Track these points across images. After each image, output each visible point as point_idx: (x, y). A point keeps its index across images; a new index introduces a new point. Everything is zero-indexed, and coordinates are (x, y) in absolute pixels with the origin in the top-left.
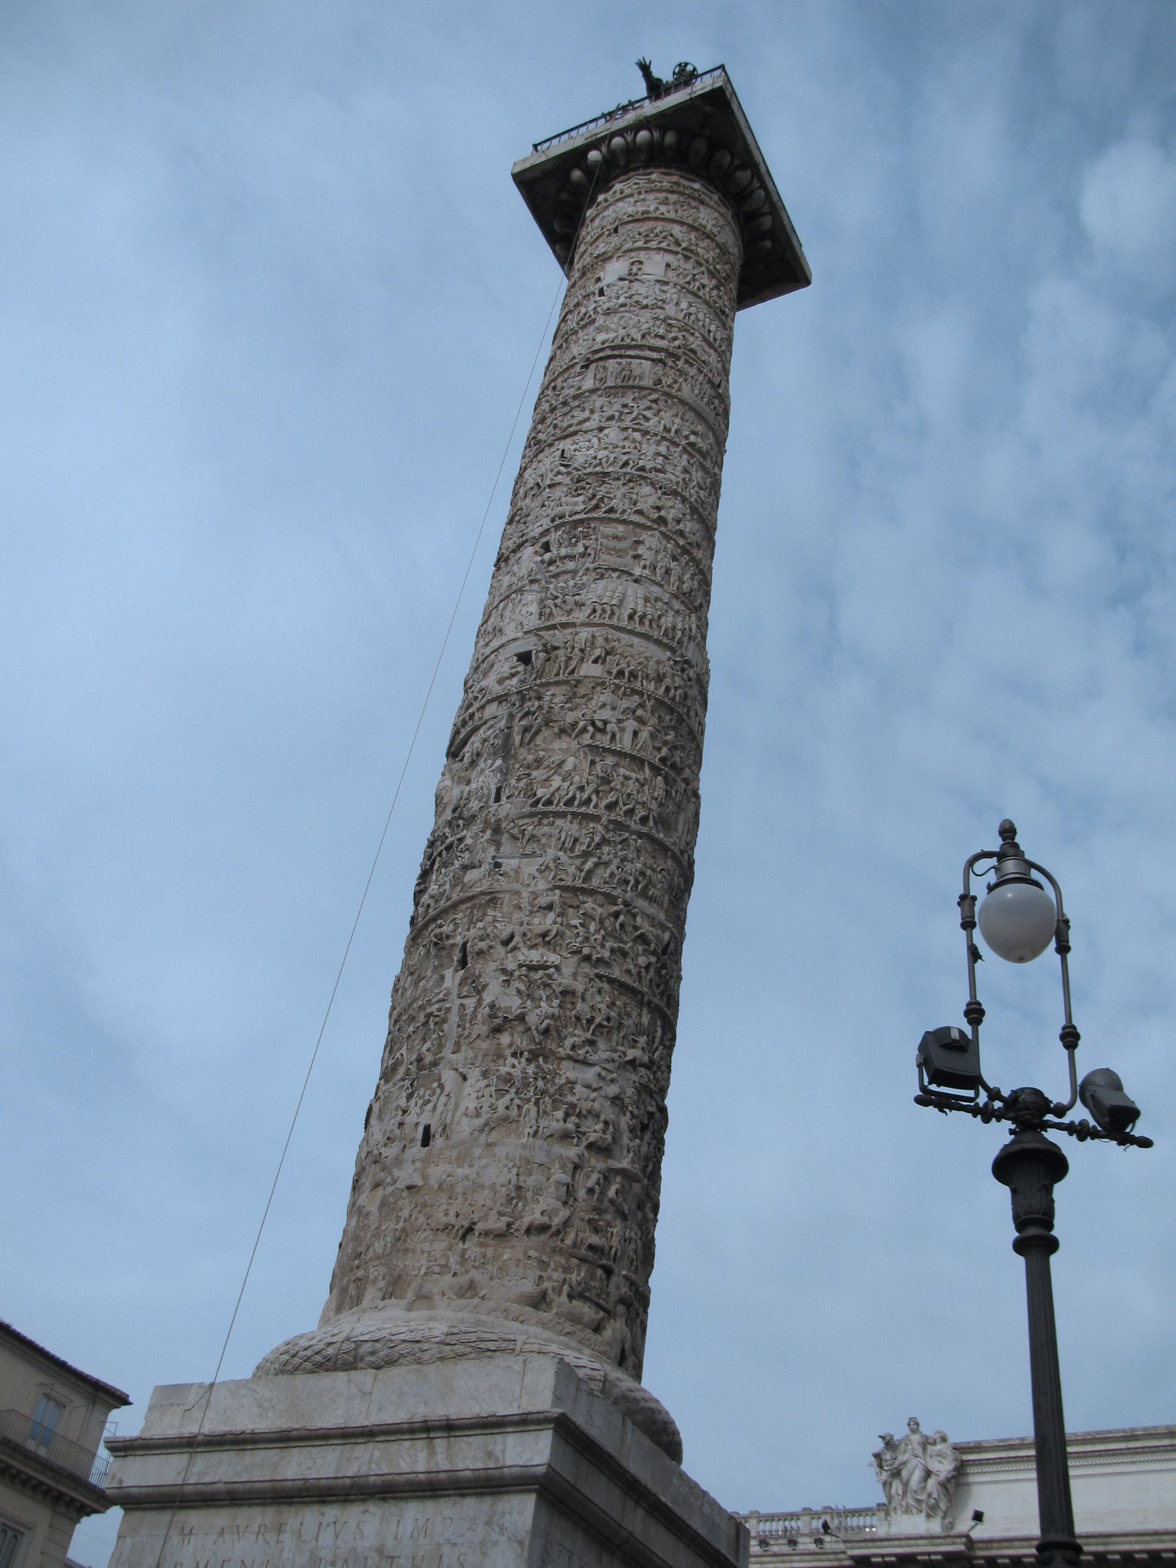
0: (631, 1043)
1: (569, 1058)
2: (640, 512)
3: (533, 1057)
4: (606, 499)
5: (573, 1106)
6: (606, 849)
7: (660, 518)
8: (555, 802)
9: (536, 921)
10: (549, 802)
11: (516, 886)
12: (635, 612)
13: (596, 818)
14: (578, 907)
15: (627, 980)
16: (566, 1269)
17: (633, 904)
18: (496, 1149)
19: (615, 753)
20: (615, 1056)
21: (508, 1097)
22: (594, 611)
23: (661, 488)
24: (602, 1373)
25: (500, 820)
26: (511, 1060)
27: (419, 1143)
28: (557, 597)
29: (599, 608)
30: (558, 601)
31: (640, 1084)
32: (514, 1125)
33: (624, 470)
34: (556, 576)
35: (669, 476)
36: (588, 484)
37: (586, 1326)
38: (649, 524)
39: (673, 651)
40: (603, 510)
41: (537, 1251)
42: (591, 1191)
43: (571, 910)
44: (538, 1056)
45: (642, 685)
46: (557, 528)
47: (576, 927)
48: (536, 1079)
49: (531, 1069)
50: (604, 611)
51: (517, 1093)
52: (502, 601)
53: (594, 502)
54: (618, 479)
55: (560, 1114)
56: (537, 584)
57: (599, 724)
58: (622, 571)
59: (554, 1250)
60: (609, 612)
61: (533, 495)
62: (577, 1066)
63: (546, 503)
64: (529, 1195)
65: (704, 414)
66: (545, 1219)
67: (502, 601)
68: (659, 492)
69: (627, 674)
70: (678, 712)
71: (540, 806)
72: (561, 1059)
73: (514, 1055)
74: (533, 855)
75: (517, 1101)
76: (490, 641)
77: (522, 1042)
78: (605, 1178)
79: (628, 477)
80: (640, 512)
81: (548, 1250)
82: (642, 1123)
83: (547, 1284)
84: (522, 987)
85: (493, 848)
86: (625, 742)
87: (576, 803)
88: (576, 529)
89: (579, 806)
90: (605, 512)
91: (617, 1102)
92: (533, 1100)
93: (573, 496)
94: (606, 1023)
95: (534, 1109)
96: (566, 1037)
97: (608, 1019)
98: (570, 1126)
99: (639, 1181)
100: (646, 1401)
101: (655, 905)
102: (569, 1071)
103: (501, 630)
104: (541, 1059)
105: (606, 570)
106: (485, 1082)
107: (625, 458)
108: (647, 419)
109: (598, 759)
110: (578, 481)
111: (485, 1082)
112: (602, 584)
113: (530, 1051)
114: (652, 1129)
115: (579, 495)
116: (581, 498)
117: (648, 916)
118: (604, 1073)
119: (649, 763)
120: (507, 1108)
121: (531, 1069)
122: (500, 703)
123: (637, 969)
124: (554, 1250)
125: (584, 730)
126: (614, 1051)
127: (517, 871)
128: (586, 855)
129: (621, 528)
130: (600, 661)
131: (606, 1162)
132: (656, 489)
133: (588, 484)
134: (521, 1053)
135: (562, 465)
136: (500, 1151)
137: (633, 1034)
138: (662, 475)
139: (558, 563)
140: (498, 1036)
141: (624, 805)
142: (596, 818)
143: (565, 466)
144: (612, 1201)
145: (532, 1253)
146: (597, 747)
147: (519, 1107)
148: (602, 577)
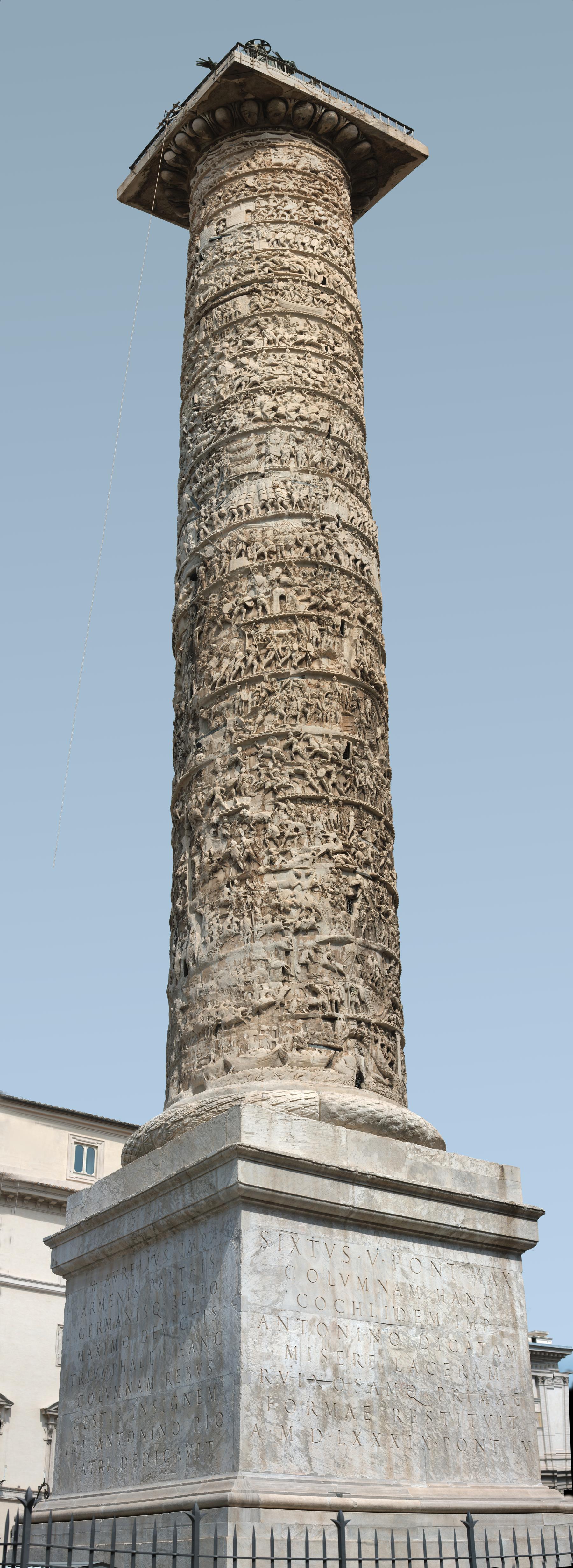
0: (324, 839)
1: (269, 871)
3: (242, 880)
5: (278, 907)
6: (272, 698)
8: (227, 680)
9: (228, 777)
10: (223, 682)
11: (211, 756)
13: (260, 679)
14: (257, 753)
15: (309, 792)
16: (293, 1030)
17: (303, 733)
18: (226, 961)
19: (265, 621)
20: (308, 855)
21: (228, 920)
23: (274, 392)
24: (317, 1099)
25: (195, 710)
26: (227, 890)
27: (183, 974)
31: (337, 868)
32: (236, 938)
33: (240, 391)
35: (281, 378)
37: (315, 1066)
38: (266, 425)
39: (309, 516)
41: (267, 1024)
42: (304, 965)
43: (252, 758)
44: (245, 879)
45: (283, 557)
47: (258, 770)
48: (246, 897)
49: (242, 890)
51: (235, 913)
55: (268, 917)
57: (249, 604)
58: (249, 473)
59: (281, 1019)
62: (277, 875)
64: (256, 986)
65: (307, 313)
66: (271, 999)
69: (266, 554)
70: (322, 563)
71: (217, 687)
72: (262, 874)
73: (228, 886)
74: (218, 728)
75: (236, 919)
77: (232, 873)
78: (316, 951)
81: (276, 1020)
82: (347, 897)
83: (279, 1046)
84: (225, 832)
85: (194, 734)
86: (275, 609)
87: (243, 672)
89: (246, 673)
91: (316, 890)
92: (246, 914)
94: (295, 833)
95: (248, 920)
96: (263, 857)
97: (297, 830)
98: (278, 923)
99: (351, 942)
100: (364, 1107)
101: (326, 724)
102: (270, 881)
104: (247, 882)
106: (213, 913)
108: (251, 343)
109: (253, 632)
111: (213, 913)
113: (238, 879)
114: (361, 897)
117: (322, 735)
118: (299, 871)
119: (299, 616)
120: (229, 927)
121: (242, 890)
122: (185, 618)
123: (318, 781)
124: (281, 1019)
125: (240, 613)
126: (308, 851)
127: (210, 745)
128: (255, 712)
129: (244, 440)
130: (243, 554)
131: (313, 939)
132: (270, 394)
134: (233, 882)
136: (229, 962)
137: (323, 832)
140: (216, 875)
141: (281, 657)
142: (260, 679)
144: (325, 966)
145: (264, 1027)
146: (250, 623)
147: (238, 923)
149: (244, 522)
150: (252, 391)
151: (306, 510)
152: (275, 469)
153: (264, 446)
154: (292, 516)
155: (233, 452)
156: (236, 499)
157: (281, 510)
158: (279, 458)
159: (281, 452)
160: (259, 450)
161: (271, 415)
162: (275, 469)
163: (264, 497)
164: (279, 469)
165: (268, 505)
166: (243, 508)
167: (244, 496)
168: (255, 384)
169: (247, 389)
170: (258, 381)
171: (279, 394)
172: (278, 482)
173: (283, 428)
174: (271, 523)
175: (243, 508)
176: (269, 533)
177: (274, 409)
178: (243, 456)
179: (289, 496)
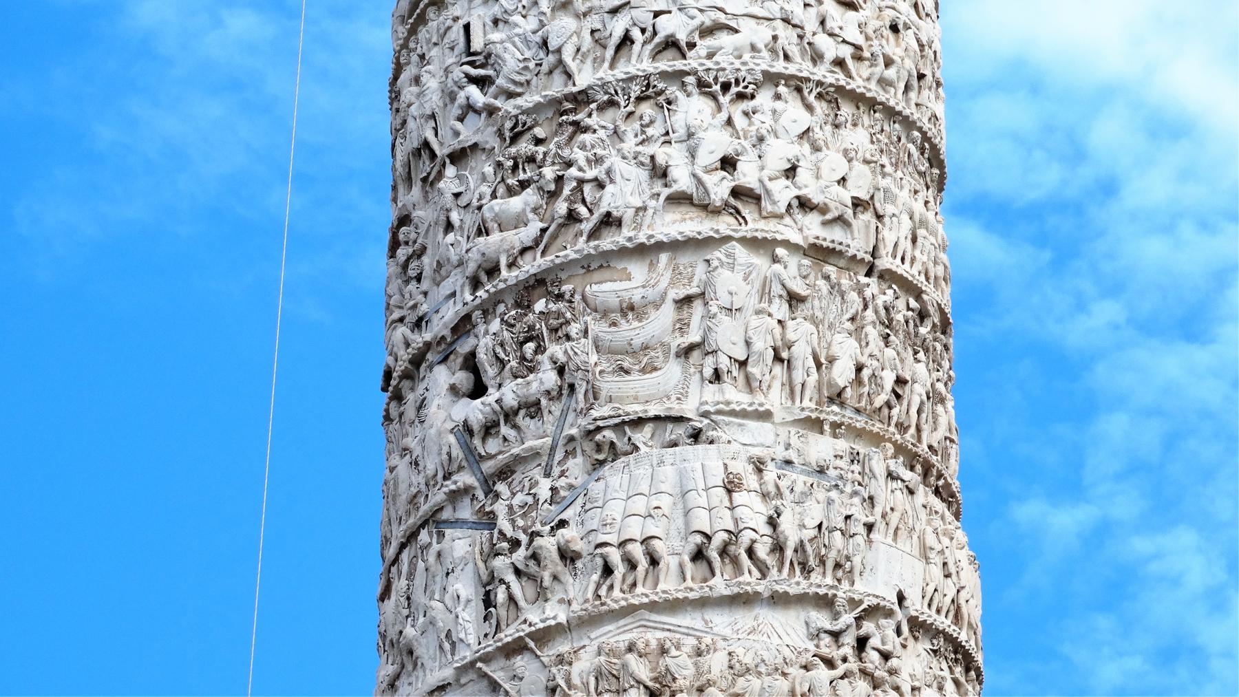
2: (680, 199)
4: (587, 188)
7: (736, 192)
12: (709, 537)
22: (608, 571)
23: (726, 87)
28: (515, 544)
29: (615, 556)
30: (521, 553)
34: (505, 473)
36: (538, 141)
40: (586, 227)
46: (487, 310)
50: (632, 565)
52: (403, 546)
53: (562, 207)
54: (612, 103)
56: (467, 501)
58: (657, 418)
60: (643, 563)
61: (424, 180)
63: (455, 217)
67: (403, 546)
68: (725, 100)
76: (397, 677)
79: (636, 90)
80: (680, 199)
88: (529, 307)
90: (594, 234)
93: (511, 192)
103: (411, 652)
105: (618, 427)
107: (618, 26)
110: (515, 139)
112: (615, 476)
115: (524, 185)
116: (530, 196)
132: (714, 97)
133: (538, 141)
135: (473, 80)
138: (723, 39)
139: (505, 430)
143: (482, 82)
148: (614, 452)
149: (642, 606)
150: (664, 75)
151: (821, 582)
152: (733, 413)
153: (698, 307)
154: (779, 600)
155: (604, 313)
156: (615, 510)
157: (750, 580)
158: (743, 364)
159: (748, 344)
160: (682, 326)
161: (719, 188)
162: (733, 413)
163: (702, 521)
164: (744, 414)
165: (713, 554)
166: (637, 551)
167: (639, 505)
168: (671, 44)
169: (647, 66)
170: (682, 37)
171: (741, 96)
172: (742, 468)
173: (754, 243)
174: (721, 621)
175: (637, 551)
176: (716, 663)
177: (728, 163)
178: (637, 342)
179: (772, 523)
